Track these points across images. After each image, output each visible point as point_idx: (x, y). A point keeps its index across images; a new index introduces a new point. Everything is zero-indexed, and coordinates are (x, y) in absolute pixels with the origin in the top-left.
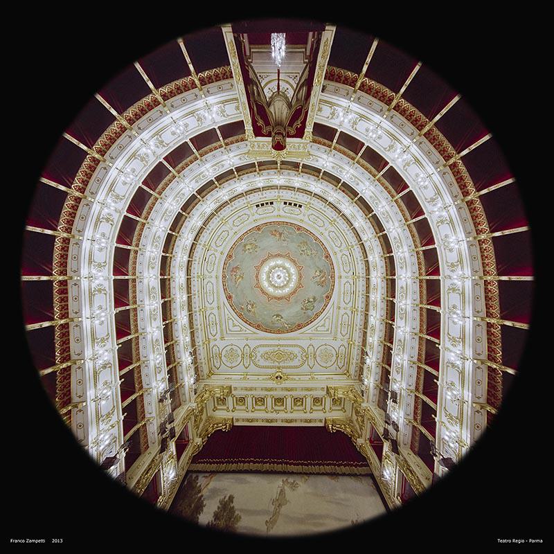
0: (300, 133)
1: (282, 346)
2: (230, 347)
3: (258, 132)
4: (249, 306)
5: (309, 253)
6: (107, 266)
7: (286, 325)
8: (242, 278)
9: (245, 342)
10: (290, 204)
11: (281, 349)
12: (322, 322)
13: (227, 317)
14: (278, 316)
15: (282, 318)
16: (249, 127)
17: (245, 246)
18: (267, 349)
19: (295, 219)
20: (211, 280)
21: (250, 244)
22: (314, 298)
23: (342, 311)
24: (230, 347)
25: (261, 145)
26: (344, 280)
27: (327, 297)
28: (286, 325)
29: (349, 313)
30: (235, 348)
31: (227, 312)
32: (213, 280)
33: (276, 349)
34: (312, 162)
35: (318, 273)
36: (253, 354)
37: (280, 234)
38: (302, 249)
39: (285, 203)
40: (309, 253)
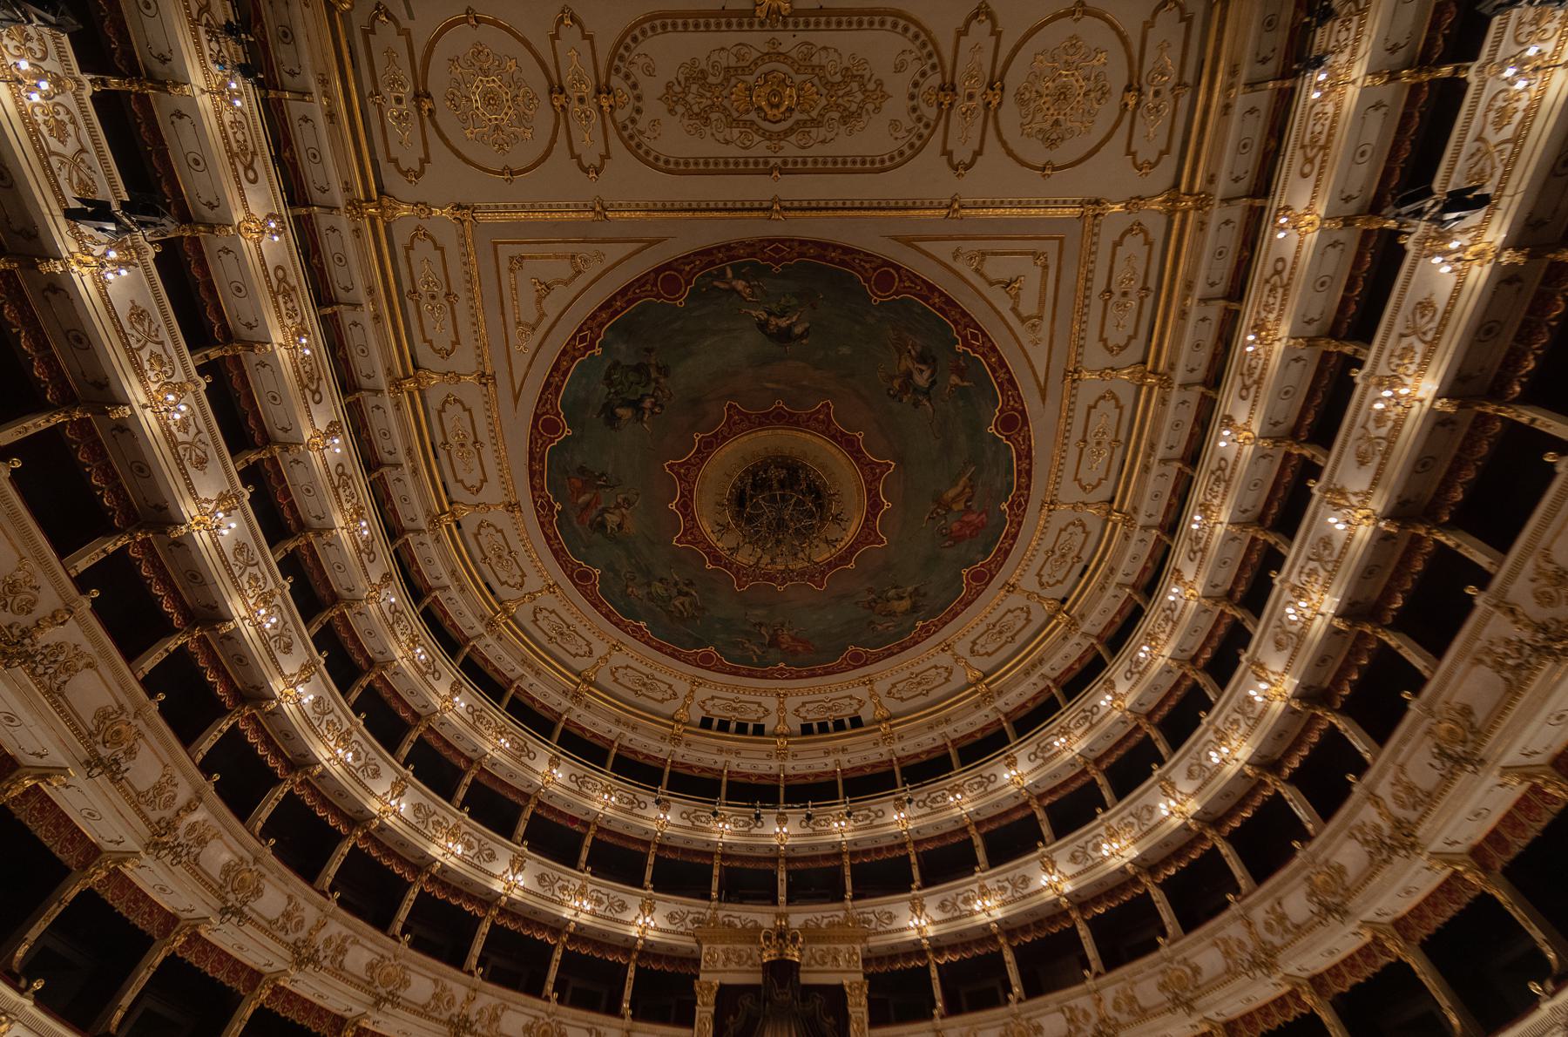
0: (727, 995)
1: (763, 168)
2: (1060, 155)
3: (836, 995)
4: (922, 379)
5: (658, 588)
6: (1478, 645)
7: (740, 285)
8: (938, 500)
9: (971, 186)
10: (742, 728)
11: (760, 148)
12: (552, 307)
13: (1044, 332)
14: (784, 336)
15: (762, 326)
16: (858, 1009)
17: (915, 608)
18: (845, 144)
19: (726, 687)
20: (1103, 358)
21: (891, 614)
22: (612, 420)
23: (464, 360)
24: (1060, 155)
25: (829, 959)
26: (493, 493)
27: (552, 427)
28: (740, 285)
29: (393, 181)
30: (1036, 152)
31: (1039, 357)
32: (1069, 492)
33: (790, 149)
34: (685, 909)
35: (612, 519)
36: (931, 113)
37: (774, 643)
38: (687, 600)
39: (759, 730)
40: (658, 588)
